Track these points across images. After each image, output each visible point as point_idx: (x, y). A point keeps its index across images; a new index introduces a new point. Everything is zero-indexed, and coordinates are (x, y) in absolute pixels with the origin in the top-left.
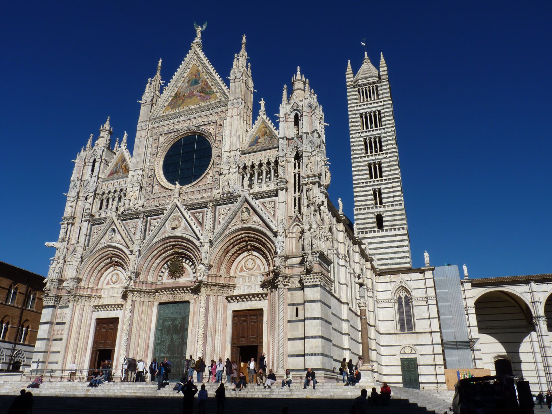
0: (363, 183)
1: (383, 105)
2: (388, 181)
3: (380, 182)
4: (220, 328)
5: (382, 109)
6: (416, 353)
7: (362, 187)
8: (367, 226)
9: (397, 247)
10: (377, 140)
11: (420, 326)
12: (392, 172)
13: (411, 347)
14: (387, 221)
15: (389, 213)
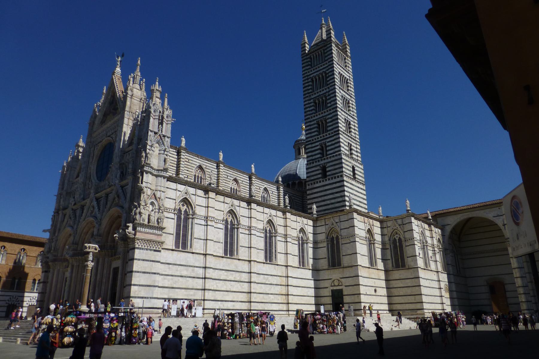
0: (313, 140)
1: (327, 67)
2: (331, 135)
3: (325, 137)
4: (105, 281)
5: (327, 70)
6: (342, 285)
7: (312, 144)
8: (315, 177)
9: (337, 193)
10: (324, 98)
11: (345, 261)
12: (334, 126)
13: (338, 280)
14: (330, 171)
15: (331, 164)
